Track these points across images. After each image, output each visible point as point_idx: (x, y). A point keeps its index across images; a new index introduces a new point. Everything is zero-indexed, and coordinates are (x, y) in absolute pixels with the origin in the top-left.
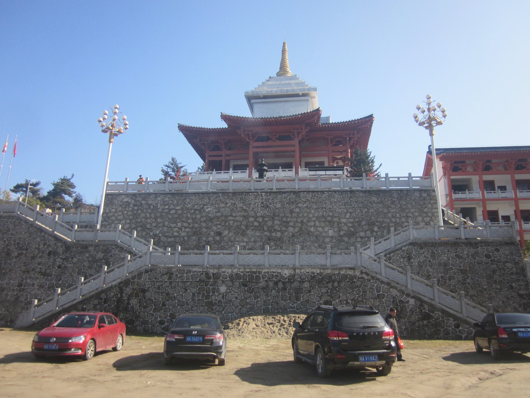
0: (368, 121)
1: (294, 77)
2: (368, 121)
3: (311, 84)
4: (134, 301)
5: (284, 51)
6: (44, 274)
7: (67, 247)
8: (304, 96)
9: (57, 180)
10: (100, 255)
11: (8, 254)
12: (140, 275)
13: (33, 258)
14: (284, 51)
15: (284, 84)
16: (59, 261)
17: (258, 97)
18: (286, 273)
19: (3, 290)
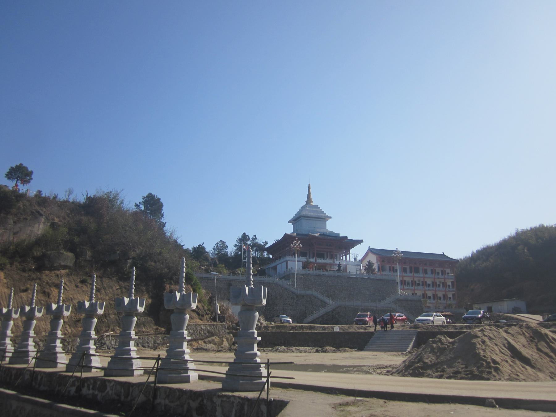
0: (361, 241)
1: (316, 207)
2: (361, 241)
3: (328, 214)
4: (337, 316)
5: (309, 189)
6: (291, 305)
7: (297, 296)
8: (323, 218)
9: (196, 245)
10: (309, 299)
11: (276, 298)
12: (337, 308)
13: (286, 299)
14: (309, 189)
15: (315, 211)
16: (295, 301)
17: (305, 217)
18: (375, 308)
19: (278, 311)
